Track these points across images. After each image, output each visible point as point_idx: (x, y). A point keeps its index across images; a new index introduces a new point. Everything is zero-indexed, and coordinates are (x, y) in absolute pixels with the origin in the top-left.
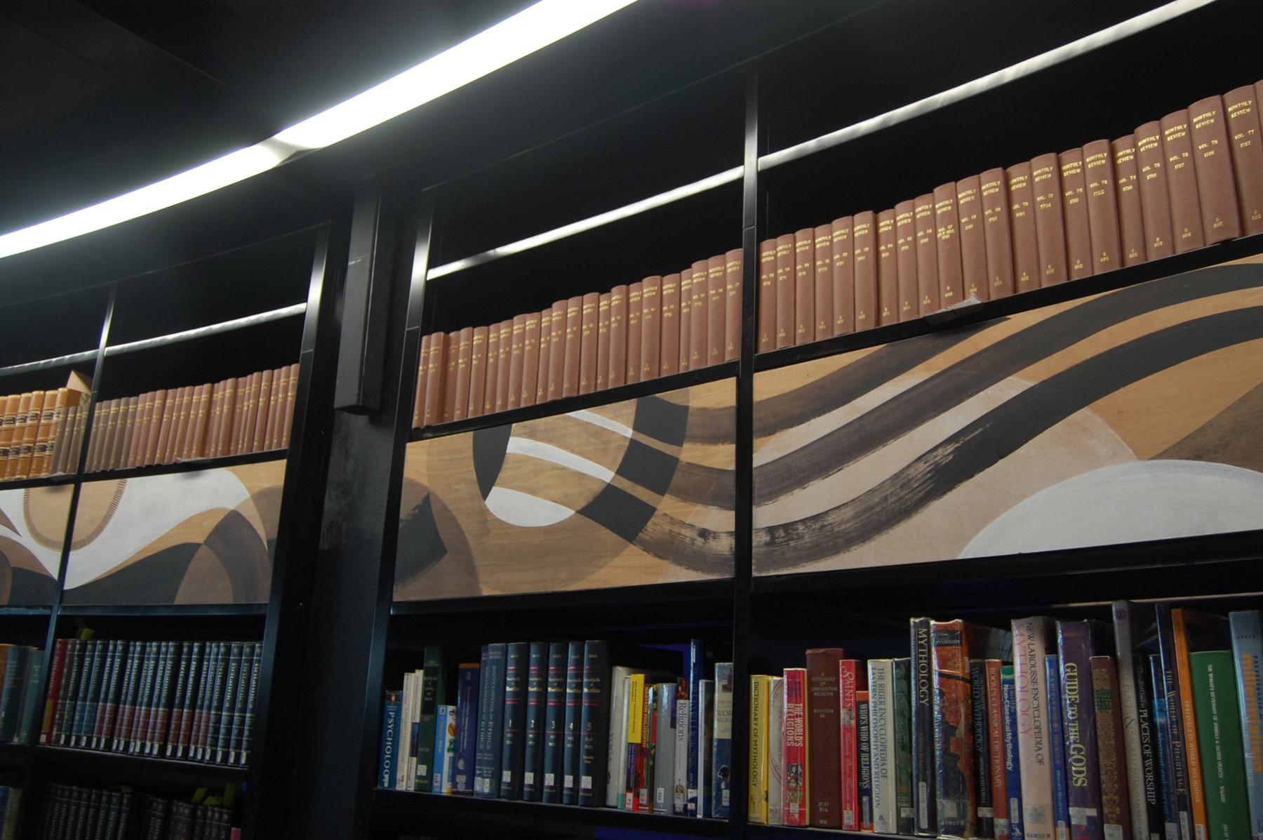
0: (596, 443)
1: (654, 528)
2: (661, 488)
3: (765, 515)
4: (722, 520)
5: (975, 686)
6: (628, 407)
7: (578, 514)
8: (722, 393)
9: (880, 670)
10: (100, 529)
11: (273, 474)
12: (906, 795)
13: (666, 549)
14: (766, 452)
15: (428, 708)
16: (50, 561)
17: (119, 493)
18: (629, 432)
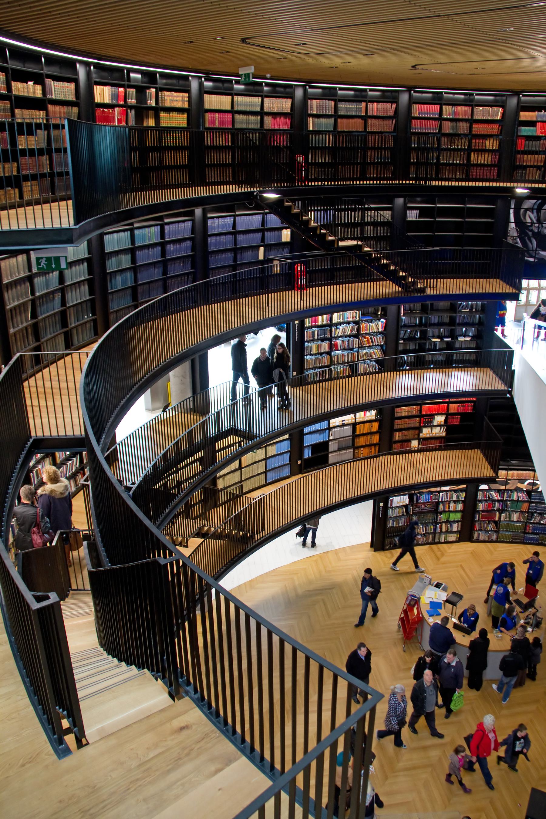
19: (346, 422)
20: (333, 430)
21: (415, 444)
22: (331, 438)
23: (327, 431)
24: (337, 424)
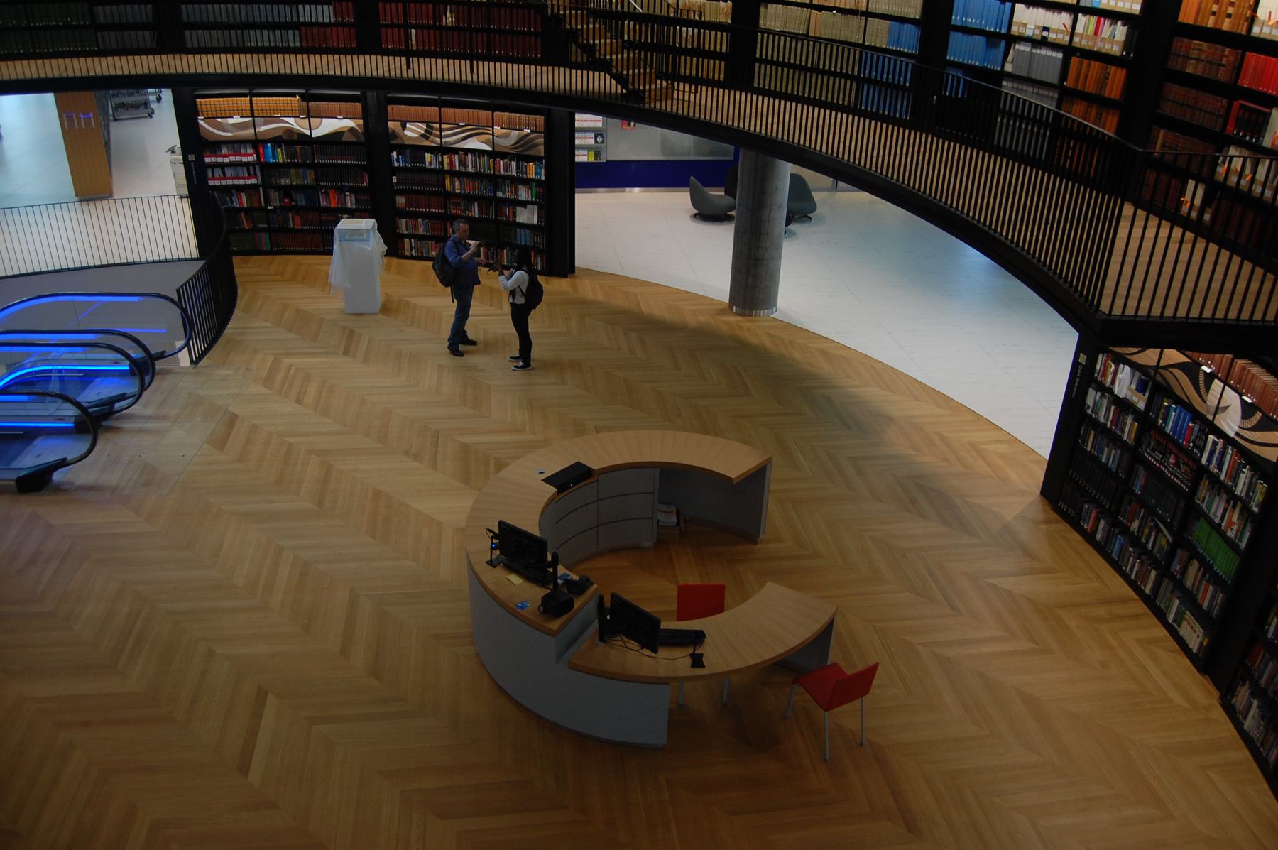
0: (421, 128)
1: (430, 139)
3: (443, 140)
4: (439, 140)
5: (465, 158)
8: (438, 126)
9: (456, 156)
10: (317, 128)
11: (361, 122)
12: (459, 166)
13: (432, 142)
14: (443, 134)
15: (398, 156)
17: (321, 121)
19: (1051, 36)
20: (1017, 47)
21: (1194, 194)
22: (1008, 68)
23: (1003, 44)
24: (1029, 33)
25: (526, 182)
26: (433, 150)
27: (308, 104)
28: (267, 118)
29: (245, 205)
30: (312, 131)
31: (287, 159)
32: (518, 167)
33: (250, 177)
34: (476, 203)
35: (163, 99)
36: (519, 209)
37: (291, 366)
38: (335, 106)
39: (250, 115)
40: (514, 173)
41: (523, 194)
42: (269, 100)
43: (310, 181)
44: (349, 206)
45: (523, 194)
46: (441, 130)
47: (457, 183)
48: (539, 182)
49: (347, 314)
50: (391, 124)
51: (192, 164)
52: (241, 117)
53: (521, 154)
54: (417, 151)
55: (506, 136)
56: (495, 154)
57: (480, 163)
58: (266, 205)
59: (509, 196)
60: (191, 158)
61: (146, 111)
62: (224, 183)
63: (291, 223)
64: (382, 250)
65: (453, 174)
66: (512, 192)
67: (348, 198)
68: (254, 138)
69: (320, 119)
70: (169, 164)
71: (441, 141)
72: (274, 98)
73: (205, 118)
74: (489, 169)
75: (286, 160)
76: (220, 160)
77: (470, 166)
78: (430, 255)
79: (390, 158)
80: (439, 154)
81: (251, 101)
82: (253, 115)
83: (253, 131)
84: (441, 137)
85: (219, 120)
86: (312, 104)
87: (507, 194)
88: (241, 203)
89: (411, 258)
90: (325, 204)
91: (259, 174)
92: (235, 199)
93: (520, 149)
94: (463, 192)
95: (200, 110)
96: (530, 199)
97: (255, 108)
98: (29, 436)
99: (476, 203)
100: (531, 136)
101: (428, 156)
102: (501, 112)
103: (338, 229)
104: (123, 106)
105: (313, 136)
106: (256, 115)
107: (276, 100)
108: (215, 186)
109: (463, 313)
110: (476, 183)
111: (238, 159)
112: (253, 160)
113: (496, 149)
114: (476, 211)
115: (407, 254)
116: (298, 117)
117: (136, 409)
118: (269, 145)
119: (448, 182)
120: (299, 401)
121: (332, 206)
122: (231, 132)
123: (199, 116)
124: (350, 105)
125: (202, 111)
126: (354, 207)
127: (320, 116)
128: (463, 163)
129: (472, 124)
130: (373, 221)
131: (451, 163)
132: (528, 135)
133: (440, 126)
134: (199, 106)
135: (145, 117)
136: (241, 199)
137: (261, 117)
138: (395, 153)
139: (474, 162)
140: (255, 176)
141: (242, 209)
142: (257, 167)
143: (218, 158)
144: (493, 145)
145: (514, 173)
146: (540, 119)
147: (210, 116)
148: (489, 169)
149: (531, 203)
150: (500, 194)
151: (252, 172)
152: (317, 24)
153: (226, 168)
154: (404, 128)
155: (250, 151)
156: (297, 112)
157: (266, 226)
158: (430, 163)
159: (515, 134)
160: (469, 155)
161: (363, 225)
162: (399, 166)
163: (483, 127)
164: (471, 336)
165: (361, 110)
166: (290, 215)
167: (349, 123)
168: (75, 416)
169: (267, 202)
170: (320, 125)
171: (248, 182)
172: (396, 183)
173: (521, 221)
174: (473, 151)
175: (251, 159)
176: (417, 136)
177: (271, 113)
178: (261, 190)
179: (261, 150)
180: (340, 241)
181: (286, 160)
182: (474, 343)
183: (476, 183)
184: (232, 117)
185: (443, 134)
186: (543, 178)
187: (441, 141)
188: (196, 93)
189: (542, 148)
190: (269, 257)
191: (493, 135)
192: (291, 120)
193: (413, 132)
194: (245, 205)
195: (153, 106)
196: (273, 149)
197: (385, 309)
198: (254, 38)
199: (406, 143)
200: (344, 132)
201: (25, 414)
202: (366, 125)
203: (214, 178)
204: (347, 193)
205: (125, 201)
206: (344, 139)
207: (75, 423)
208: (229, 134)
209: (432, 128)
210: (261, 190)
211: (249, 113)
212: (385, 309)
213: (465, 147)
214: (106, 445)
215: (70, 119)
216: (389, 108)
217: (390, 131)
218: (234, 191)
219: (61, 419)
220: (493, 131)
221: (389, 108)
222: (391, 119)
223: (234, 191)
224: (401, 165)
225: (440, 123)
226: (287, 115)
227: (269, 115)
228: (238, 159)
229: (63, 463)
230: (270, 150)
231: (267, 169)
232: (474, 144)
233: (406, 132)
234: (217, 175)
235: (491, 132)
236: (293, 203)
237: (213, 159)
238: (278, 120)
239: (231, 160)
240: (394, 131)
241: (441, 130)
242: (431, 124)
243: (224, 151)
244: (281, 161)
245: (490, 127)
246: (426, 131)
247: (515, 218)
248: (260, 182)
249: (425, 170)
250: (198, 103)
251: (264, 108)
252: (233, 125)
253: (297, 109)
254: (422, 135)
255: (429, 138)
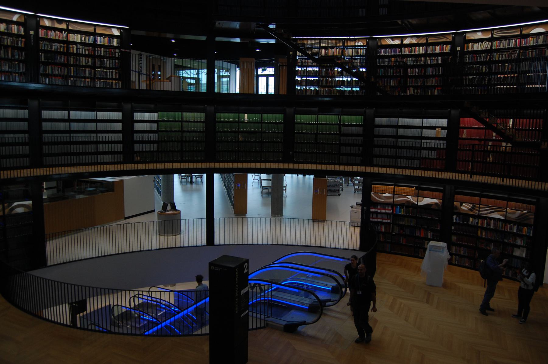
0: (470, 206)
2: (474, 209)
5: (490, 222)
6: (472, 204)
7: (469, 210)
8: (478, 206)
9: (486, 220)
11: (441, 201)
12: (486, 225)
13: (475, 213)
15: (456, 218)
16: (416, 203)
17: (423, 199)
18: (472, 206)
25: (521, 236)
26: (474, 217)
27: (418, 191)
28: (399, 196)
29: (383, 231)
30: (418, 203)
31: (405, 213)
32: (517, 229)
33: (387, 219)
34: (493, 244)
35: (344, 190)
36: (515, 249)
37: (401, 303)
38: (431, 193)
39: (392, 193)
40: (515, 231)
41: (519, 242)
42: (402, 188)
43: (413, 224)
44: (429, 237)
45: (519, 242)
46: (479, 208)
47: (484, 233)
48: (528, 237)
49: (427, 285)
50: (455, 203)
51: (365, 211)
52: (389, 194)
53: (520, 222)
54: (466, 216)
55: (514, 213)
56: (506, 221)
57: (497, 225)
58: (392, 232)
59: (511, 242)
60: (365, 208)
61: (338, 193)
62: (376, 220)
63: (401, 241)
64: (448, 258)
65: (482, 228)
66: (512, 240)
67: (429, 234)
68: (392, 203)
69: (423, 198)
70: (350, 212)
71: (479, 213)
72: (404, 187)
73: (374, 193)
74: (502, 228)
75: (404, 214)
76: (376, 210)
77: (492, 226)
78: (465, 265)
79: (452, 218)
80: (477, 219)
81: (394, 189)
82: (394, 194)
83: (393, 200)
84: (479, 211)
85: (380, 194)
86: (420, 191)
87: (510, 241)
88: (381, 230)
89: (455, 265)
90: (418, 235)
91: (392, 218)
92: (379, 227)
93: (520, 220)
94: (486, 237)
95: (372, 189)
96: (522, 244)
97: (395, 191)
98: (289, 308)
99: (493, 244)
100: (527, 214)
101: (471, 219)
102: (512, 202)
103: (430, 245)
104: (330, 190)
105: (418, 205)
106: (395, 194)
107: (405, 188)
108: (372, 221)
109: (489, 294)
110: (494, 234)
111: (384, 211)
112: (390, 212)
113: (507, 219)
114: (492, 247)
115: (454, 263)
116: (413, 196)
117: (333, 307)
118: (398, 207)
119: (479, 232)
120: (406, 320)
121: (421, 236)
122: (383, 200)
123: (372, 192)
124: (438, 193)
125: (373, 190)
126: (431, 238)
127: (423, 197)
128: (489, 224)
129: (495, 206)
130: (446, 244)
131: (483, 223)
132: (526, 213)
133: (479, 206)
134: (373, 188)
135: (337, 196)
136: (382, 227)
137: (397, 195)
138: (455, 216)
139: (494, 224)
140: (390, 219)
141: (381, 232)
142: (391, 216)
143: (376, 210)
144: (505, 216)
145: (515, 231)
146: (533, 207)
147: (376, 192)
148: (502, 228)
149: (523, 247)
150: (506, 241)
151: (389, 217)
152: (428, 159)
153: (378, 214)
154: (461, 205)
155: (390, 208)
156: (413, 194)
157: (390, 241)
158: (472, 222)
159: (518, 212)
160: (492, 221)
161: (441, 245)
162: (456, 222)
163: (502, 208)
164: (491, 306)
165: (442, 196)
166: (402, 238)
167: (435, 201)
168: (310, 304)
169: (393, 231)
170: (422, 201)
171: (386, 221)
172: (454, 230)
173: (516, 255)
174: (495, 219)
175: (389, 212)
176: (467, 209)
177: (402, 193)
178: (391, 225)
179: (395, 208)
180: (430, 250)
181: (404, 214)
182: (493, 310)
183: (494, 234)
184: (385, 194)
185: (480, 209)
186: (531, 235)
187: (479, 213)
188: (373, 182)
189: (532, 220)
190: (389, 255)
191: (506, 212)
192: (410, 197)
193: (465, 207)
194: (383, 231)
195: (340, 192)
196: (400, 209)
197: (445, 286)
198: (401, 162)
199: (461, 212)
200: (432, 205)
201: (290, 299)
202: (443, 202)
203: (372, 218)
204: (429, 232)
205: (335, 222)
206: (432, 208)
207: (309, 307)
208: (383, 200)
209: (475, 206)
210: (391, 225)
211: (392, 193)
212: (445, 286)
213: (491, 216)
214: (324, 320)
215: (317, 190)
216: (456, 196)
217: (454, 206)
218: (380, 224)
219: (304, 304)
220: (506, 210)
221: (456, 196)
222: (456, 201)
223: (380, 224)
224: (457, 222)
225: (480, 204)
226: (408, 195)
227: (401, 194)
228: (384, 211)
229: (304, 323)
230: (398, 209)
231: (395, 217)
232: (496, 215)
233: (462, 207)
234: (374, 217)
235: (505, 211)
236: (404, 233)
237: (374, 210)
238: (404, 196)
239: (381, 211)
240: (456, 207)
241: (479, 208)
242: (475, 205)
243: (379, 207)
244: (402, 214)
245: (505, 208)
246: (472, 207)
247: (513, 253)
248: (391, 222)
249: (469, 225)
250: (372, 187)
251: (399, 191)
252: (385, 197)
253: (413, 193)
254: (470, 209)
255: (473, 210)
